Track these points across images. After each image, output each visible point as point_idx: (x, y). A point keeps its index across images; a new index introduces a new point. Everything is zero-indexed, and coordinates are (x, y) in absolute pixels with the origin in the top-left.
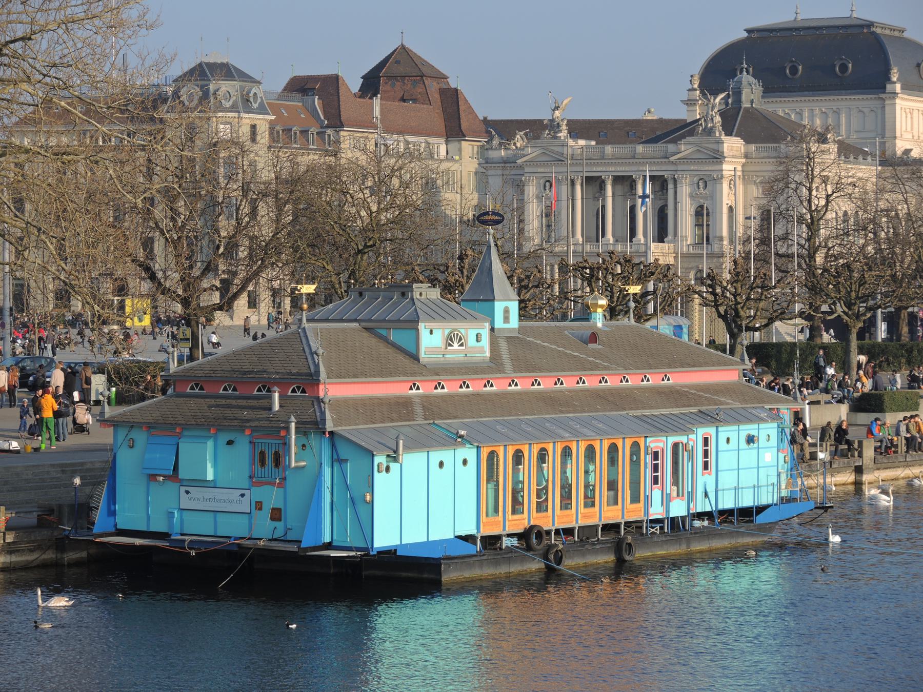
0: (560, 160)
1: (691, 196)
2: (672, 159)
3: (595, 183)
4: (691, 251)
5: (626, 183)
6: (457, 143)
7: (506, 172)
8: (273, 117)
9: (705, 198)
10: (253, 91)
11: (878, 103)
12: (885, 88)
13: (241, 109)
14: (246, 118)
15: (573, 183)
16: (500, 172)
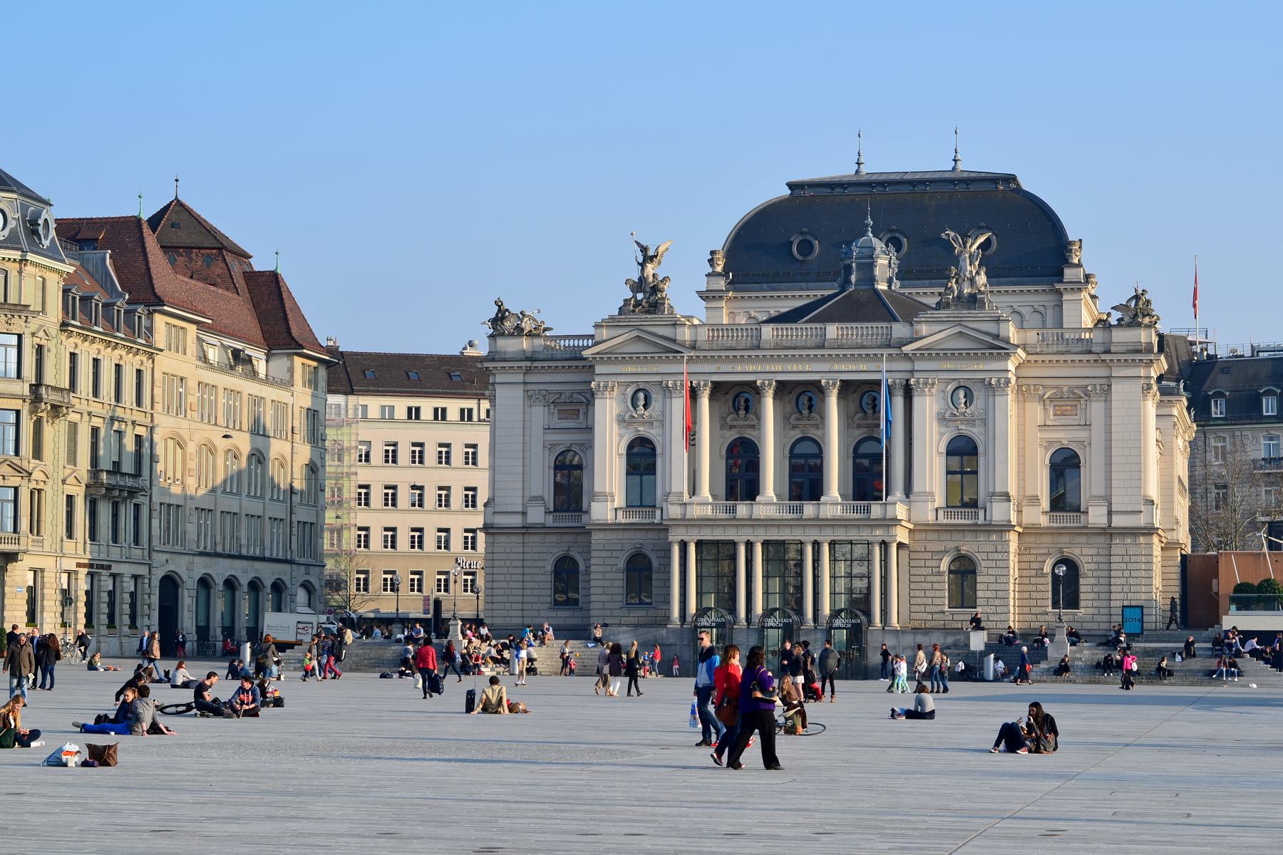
0: (670, 350)
1: (942, 419)
2: (906, 349)
3: (737, 399)
4: (942, 519)
5: (801, 398)
6: (285, 359)
7: (530, 378)
8: (71, 269)
9: (971, 422)
10: (44, 215)
11: (1048, 300)
12: (1061, 274)
13: (25, 246)
14: (33, 263)
15: (694, 394)
16: (520, 378)
